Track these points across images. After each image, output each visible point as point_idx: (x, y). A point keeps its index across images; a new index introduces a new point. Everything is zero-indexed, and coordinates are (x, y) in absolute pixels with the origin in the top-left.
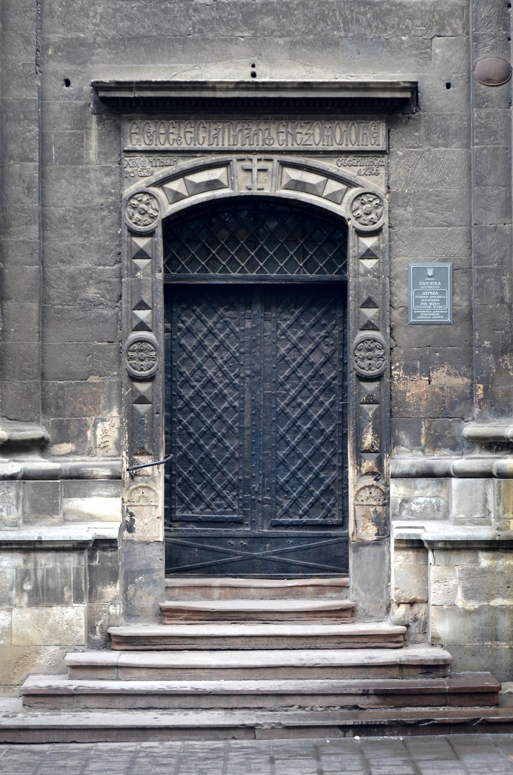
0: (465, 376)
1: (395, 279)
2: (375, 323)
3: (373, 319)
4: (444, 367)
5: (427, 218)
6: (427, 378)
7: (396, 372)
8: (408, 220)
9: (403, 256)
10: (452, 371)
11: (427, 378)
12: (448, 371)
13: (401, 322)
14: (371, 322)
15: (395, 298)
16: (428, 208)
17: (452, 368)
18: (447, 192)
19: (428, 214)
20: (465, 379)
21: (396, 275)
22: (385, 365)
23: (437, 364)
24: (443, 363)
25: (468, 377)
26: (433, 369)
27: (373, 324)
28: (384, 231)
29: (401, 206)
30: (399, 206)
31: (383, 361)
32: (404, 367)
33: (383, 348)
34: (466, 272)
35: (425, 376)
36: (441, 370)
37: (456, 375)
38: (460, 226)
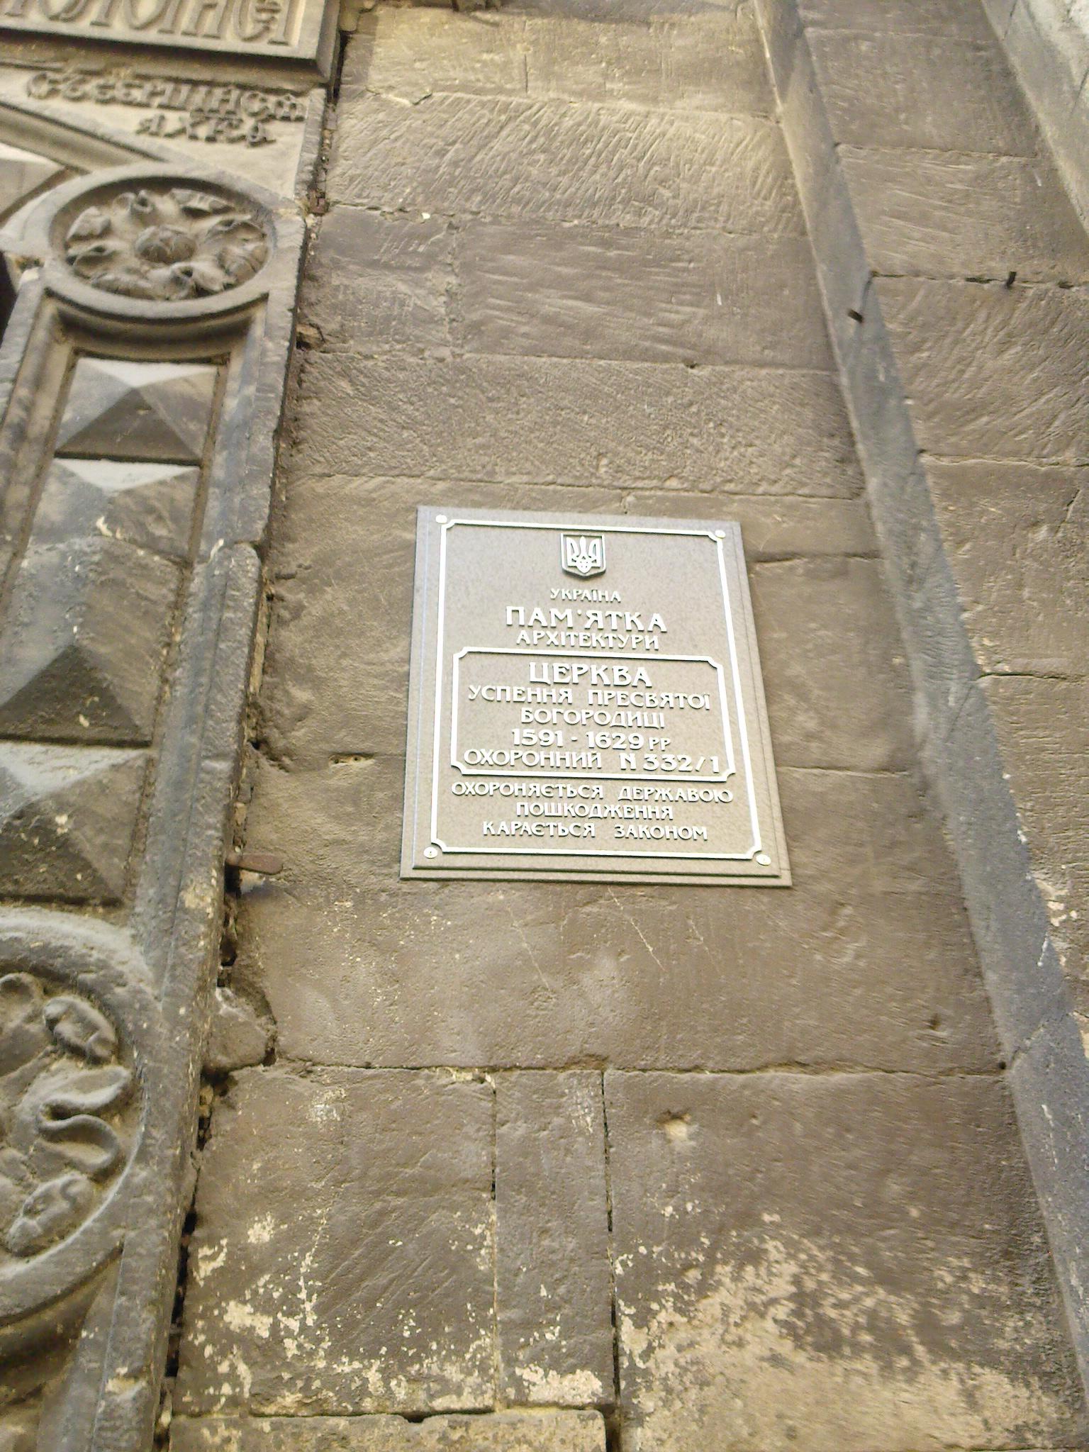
0: (991, 1359)
1: (313, 581)
2: (89, 843)
3: (78, 814)
4: (755, 1257)
5: (549, 320)
6: (587, 1385)
7: (237, 1315)
8: (432, 320)
9: (379, 470)
10: (851, 1302)
11: (587, 1385)
12: (803, 1299)
13: (336, 861)
14: (45, 829)
15: (302, 695)
16: (561, 284)
17: (843, 1275)
18: (668, 235)
19: (553, 303)
20: (992, 1381)
21: (325, 560)
22: (113, 1218)
23: (682, 1234)
24: (747, 1218)
25: (1022, 1367)
26: (642, 1286)
27: (63, 849)
28: (257, 331)
29: (387, 266)
30: (374, 264)
31: (102, 1176)
32: (335, 1252)
33: (120, 1051)
34: (842, 573)
35: (558, 1363)
36: (727, 1294)
37: (889, 1345)
38: (762, 365)
